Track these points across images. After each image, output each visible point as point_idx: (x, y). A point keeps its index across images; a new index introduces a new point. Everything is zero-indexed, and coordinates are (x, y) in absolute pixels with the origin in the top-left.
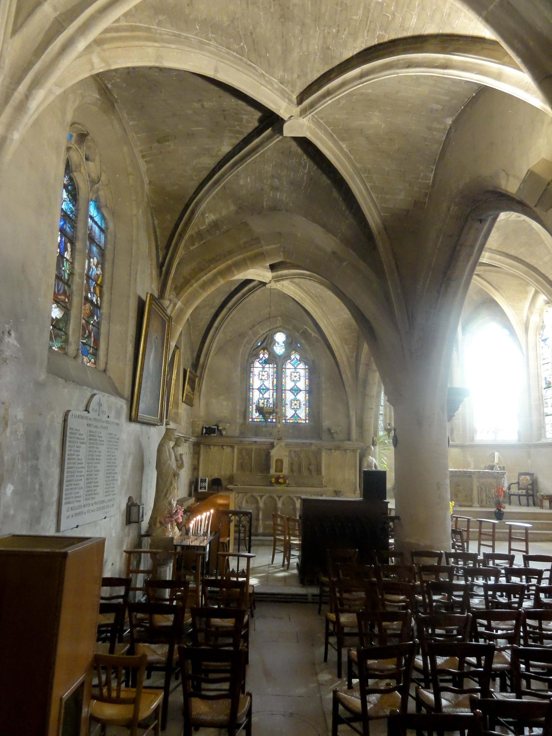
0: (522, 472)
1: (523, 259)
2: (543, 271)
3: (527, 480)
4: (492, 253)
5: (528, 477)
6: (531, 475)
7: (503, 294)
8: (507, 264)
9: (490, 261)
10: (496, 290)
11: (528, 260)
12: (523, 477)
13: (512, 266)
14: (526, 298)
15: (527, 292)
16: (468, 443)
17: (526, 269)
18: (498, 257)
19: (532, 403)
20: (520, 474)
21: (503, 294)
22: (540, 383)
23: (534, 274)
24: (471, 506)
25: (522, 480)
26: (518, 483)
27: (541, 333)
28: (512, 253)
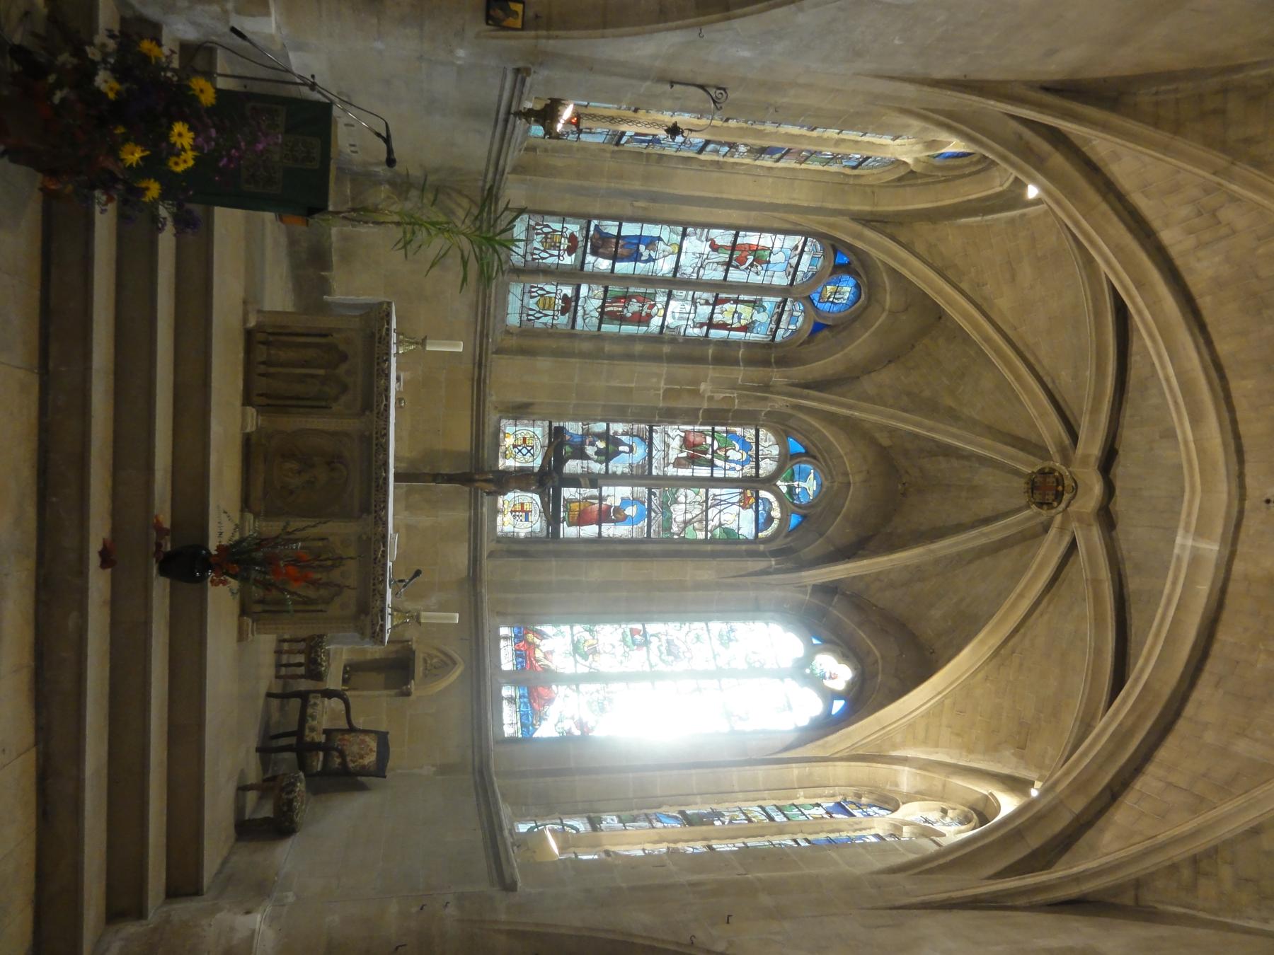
0: (394, 749)
1: (1206, 678)
2: (1162, 754)
3: (362, 757)
4: (1217, 566)
5: (370, 759)
6: (380, 770)
7: (980, 676)
8: (1176, 621)
9: (1186, 558)
10: (997, 652)
11: (1203, 691)
12: (374, 745)
13: (1171, 640)
14: (971, 751)
15: (992, 749)
16: (486, 596)
17: (1166, 692)
18: (1204, 588)
19: (631, 775)
20: (382, 738)
21: (980, 676)
22: (698, 799)
23: (1148, 724)
24: (246, 503)
25: (363, 742)
26: (352, 729)
27: (864, 800)
28: (1226, 637)
